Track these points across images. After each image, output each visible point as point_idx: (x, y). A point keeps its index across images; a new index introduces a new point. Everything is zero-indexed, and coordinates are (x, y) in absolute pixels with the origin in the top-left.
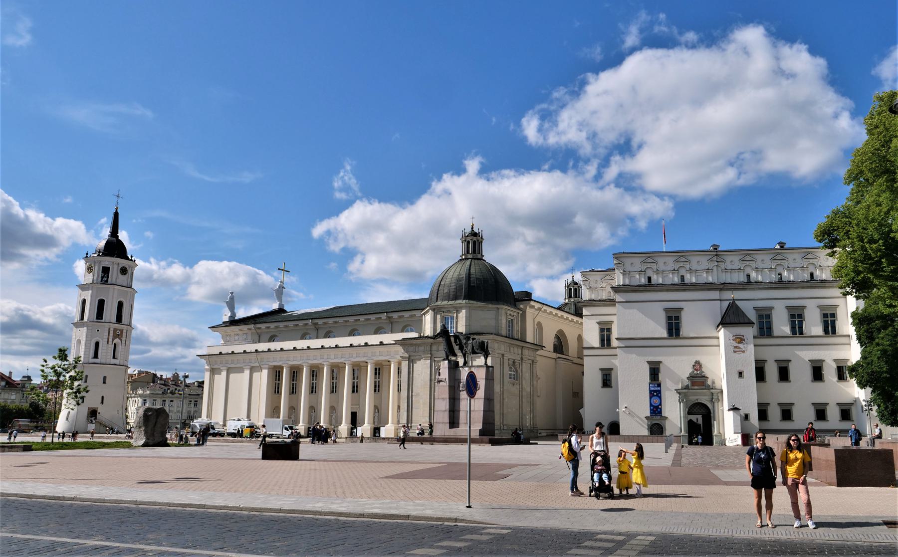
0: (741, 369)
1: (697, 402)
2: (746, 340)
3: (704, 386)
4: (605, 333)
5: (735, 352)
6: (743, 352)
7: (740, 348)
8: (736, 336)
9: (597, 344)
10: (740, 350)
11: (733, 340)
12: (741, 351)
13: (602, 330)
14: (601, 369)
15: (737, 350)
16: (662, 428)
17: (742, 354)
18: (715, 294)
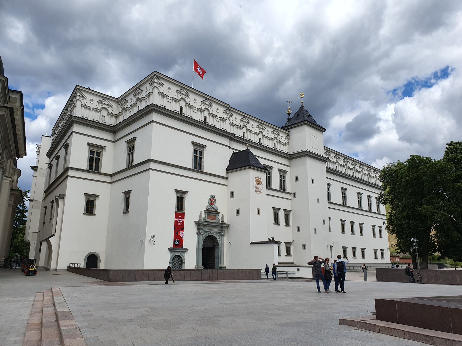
0: (259, 207)
1: (210, 234)
2: (262, 182)
3: (215, 219)
4: (95, 156)
5: (256, 191)
6: (261, 192)
7: (259, 189)
8: (257, 178)
9: (85, 166)
10: (259, 190)
11: (255, 181)
12: (259, 192)
13: (92, 153)
14: (86, 194)
15: (257, 190)
16: (181, 260)
17: (260, 194)
18: (226, 141)
